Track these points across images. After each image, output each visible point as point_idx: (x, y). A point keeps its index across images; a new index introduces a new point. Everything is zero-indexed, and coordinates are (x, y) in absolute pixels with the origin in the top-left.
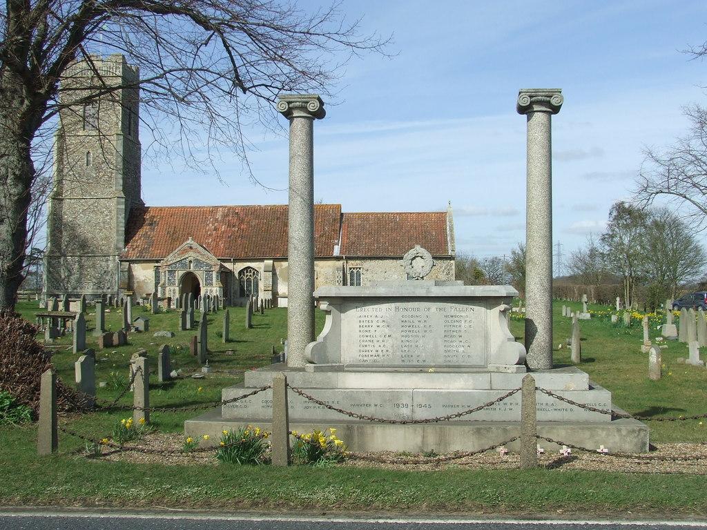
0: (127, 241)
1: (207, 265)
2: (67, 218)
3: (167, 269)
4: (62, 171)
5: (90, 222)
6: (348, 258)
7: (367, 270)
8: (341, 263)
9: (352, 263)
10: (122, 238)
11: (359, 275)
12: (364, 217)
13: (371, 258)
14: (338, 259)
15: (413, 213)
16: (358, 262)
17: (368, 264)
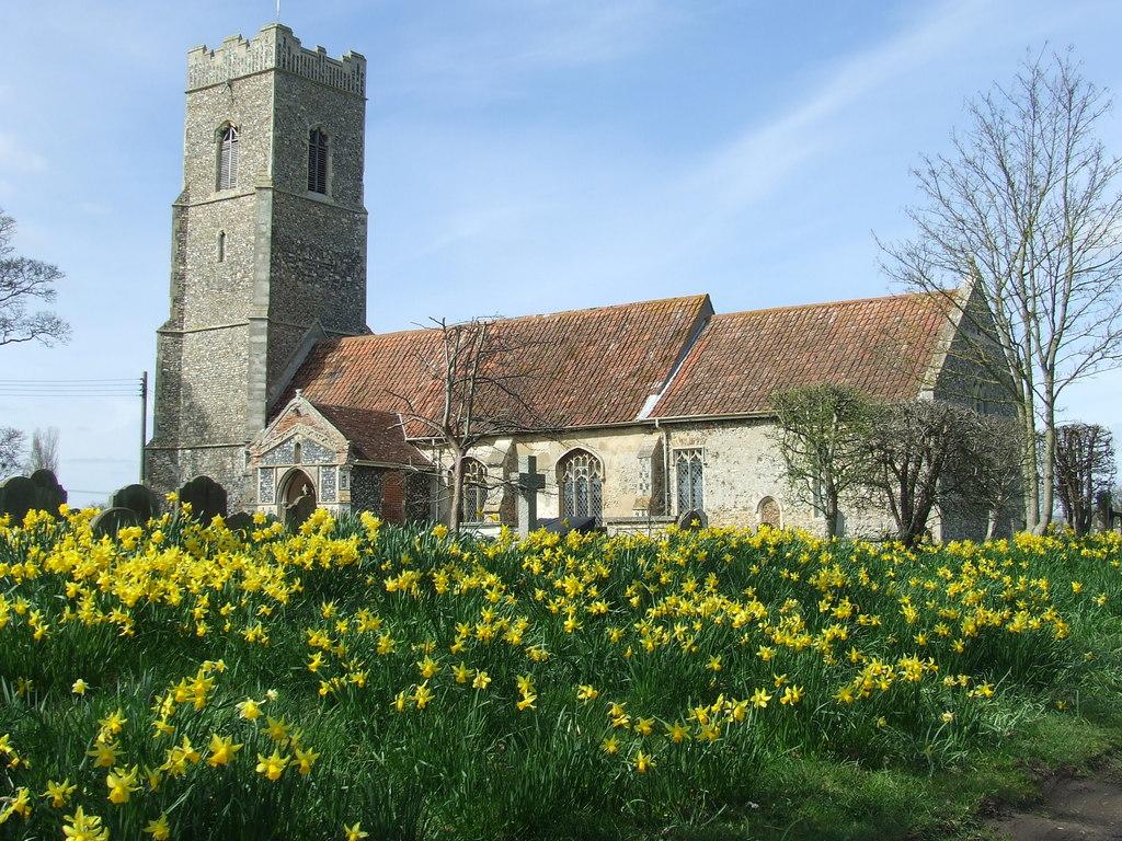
0: (272, 412)
1: (326, 452)
2: (188, 373)
3: (260, 465)
4: (183, 277)
5: (220, 375)
6: (669, 426)
7: (717, 455)
8: (650, 441)
9: (680, 440)
10: (261, 405)
11: (697, 468)
12: (753, 321)
13: (723, 423)
14: (647, 427)
15: (877, 301)
16: (695, 434)
17: (717, 439)
